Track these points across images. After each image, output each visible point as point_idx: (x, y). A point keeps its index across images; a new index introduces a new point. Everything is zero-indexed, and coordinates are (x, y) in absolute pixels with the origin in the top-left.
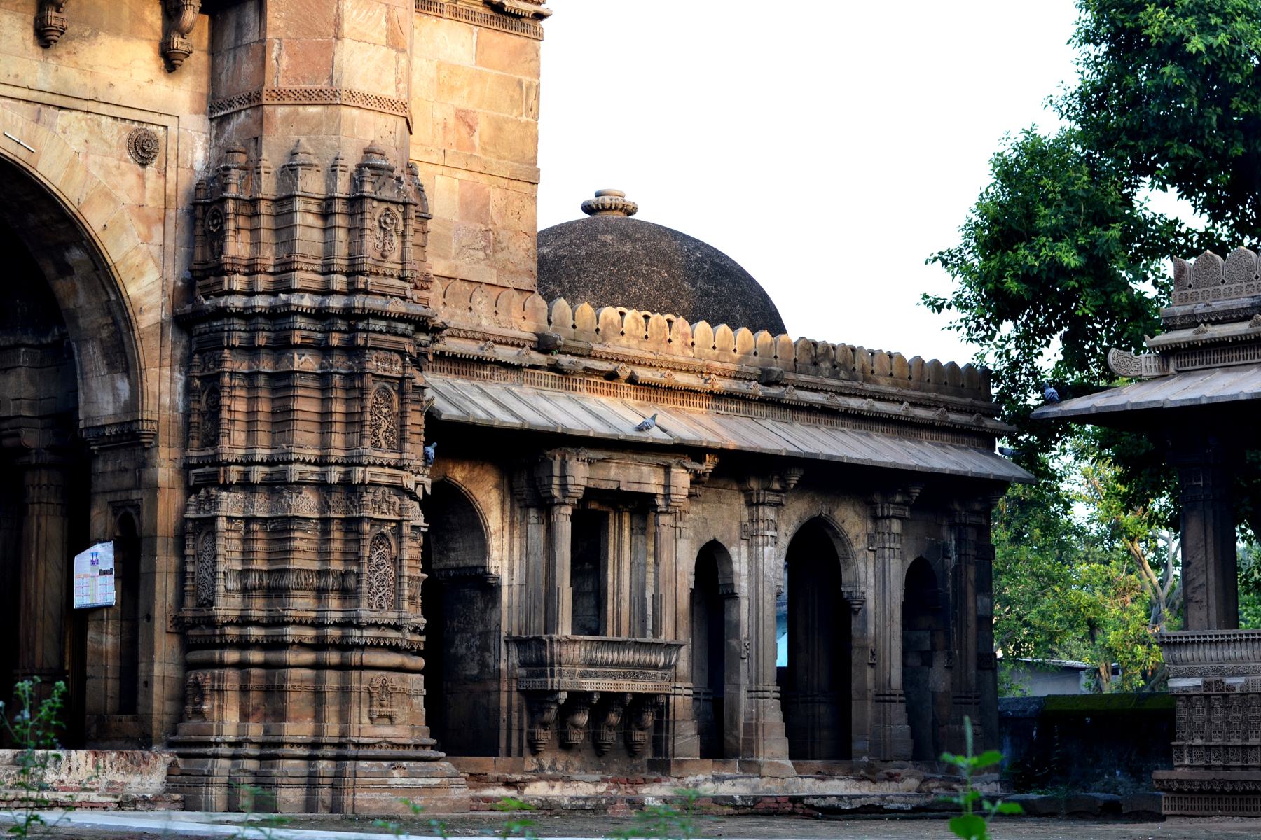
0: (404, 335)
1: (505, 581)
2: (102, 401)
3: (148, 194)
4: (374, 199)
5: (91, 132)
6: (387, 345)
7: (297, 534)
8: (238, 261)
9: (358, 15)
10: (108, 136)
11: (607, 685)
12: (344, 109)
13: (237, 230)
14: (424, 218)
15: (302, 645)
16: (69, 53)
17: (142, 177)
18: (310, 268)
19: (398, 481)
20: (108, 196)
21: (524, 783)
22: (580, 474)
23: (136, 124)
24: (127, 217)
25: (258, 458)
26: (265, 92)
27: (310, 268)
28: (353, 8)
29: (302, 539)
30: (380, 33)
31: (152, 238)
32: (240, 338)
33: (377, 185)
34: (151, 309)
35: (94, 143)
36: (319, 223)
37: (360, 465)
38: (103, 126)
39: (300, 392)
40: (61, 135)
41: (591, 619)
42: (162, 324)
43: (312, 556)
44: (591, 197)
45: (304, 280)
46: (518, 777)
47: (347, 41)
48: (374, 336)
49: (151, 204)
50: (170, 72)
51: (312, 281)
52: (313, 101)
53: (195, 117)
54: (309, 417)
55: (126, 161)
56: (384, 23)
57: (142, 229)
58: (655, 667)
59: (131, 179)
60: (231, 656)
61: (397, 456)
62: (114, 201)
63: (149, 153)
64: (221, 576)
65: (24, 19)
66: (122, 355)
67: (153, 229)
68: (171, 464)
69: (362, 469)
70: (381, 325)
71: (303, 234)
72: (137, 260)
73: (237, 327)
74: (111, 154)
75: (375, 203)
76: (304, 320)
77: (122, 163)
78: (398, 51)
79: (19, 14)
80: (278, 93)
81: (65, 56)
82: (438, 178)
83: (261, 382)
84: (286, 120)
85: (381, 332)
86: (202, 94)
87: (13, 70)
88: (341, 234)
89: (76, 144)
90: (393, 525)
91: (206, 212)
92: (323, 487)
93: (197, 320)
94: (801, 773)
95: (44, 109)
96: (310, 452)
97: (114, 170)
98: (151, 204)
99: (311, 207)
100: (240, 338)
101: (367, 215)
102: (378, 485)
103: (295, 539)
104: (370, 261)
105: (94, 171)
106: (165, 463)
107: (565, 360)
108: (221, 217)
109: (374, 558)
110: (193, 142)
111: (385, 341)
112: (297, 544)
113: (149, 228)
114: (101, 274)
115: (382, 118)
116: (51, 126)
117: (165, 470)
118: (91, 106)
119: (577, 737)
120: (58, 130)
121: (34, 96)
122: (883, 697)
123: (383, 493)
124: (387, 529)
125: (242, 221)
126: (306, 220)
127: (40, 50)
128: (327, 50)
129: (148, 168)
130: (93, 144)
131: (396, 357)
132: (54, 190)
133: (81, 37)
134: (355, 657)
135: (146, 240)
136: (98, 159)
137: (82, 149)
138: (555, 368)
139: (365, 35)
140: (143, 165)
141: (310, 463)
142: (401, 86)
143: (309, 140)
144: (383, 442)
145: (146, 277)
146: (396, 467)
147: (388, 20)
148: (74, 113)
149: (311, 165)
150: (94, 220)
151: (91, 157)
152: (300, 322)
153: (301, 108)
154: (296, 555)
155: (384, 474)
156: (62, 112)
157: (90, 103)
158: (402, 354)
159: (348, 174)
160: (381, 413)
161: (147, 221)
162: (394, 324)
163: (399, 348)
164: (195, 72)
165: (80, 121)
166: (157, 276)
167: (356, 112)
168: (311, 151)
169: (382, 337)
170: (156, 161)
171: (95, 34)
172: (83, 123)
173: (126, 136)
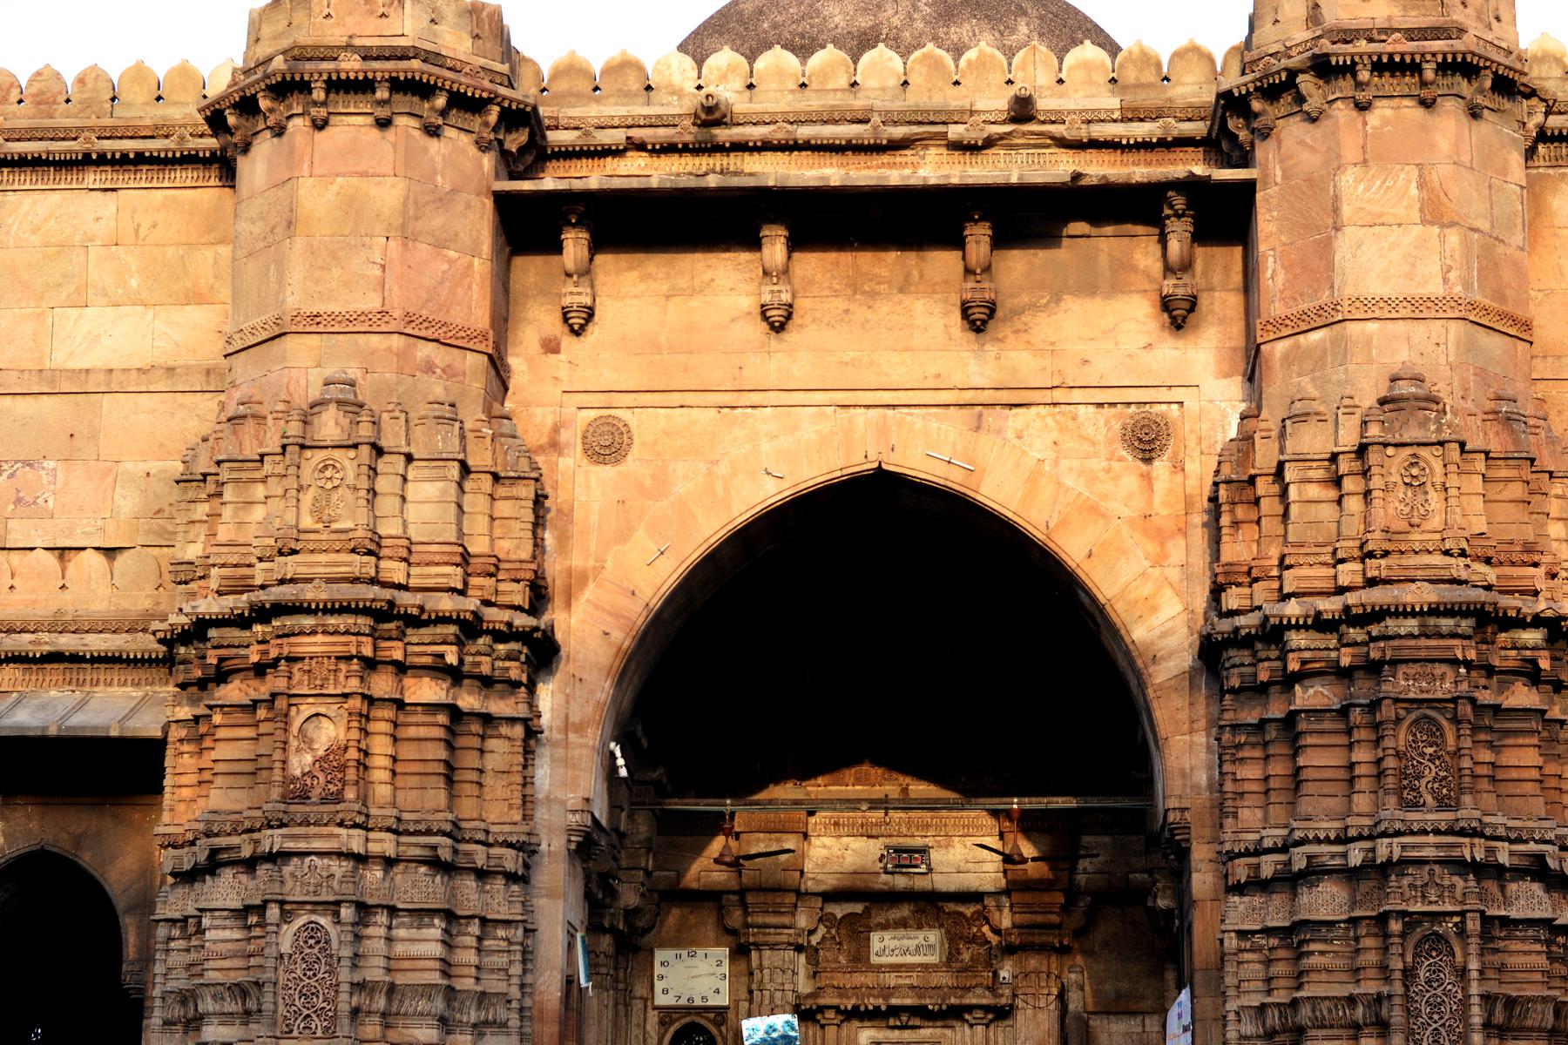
0: (1454, 636)
3: (1157, 499)
4: (1386, 445)
5: (1061, 430)
6: (1423, 654)
7: (1313, 947)
8: (1235, 569)
9: (1366, 190)
10: (1091, 430)
12: (1351, 326)
13: (1236, 524)
16: (1017, 332)
17: (1147, 478)
18: (1311, 560)
19: (1456, 853)
20: (1093, 510)
23: (1133, 407)
24: (1126, 532)
25: (1268, 843)
26: (1259, 327)
27: (1311, 560)
28: (1358, 181)
29: (1322, 953)
30: (1410, 207)
31: (1166, 557)
32: (1241, 675)
33: (1397, 425)
34: (1170, 655)
35: (1067, 444)
36: (1332, 494)
37: (1384, 834)
38: (1081, 419)
39: (1310, 740)
40: (1016, 442)
42: (1192, 674)
43: (1344, 977)
45: (1299, 578)
47: (1348, 230)
48: (1396, 643)
49: (1164, 512)
50: (1179, 327)
51: (1316, 578)
52: (1314, 325)
53: (1226, 381)
54: (1329, 774)
55: (1121, 459)
56: (1414, 191)
57: (1151, 547)
59: (1130, 482)
61: (1449, 816)
62: (1104, 516)
63: (1149, 442)
64: (1231, 1016)
65: (946, 301)
67: (1170, 545)
68: (1213, 866)
69: (1386, 841)
70: (1411, 625)
71: (1301, 514)
72: (1146, 590)
73: (1237, 661)
74: (1096, 455)
75: (1390, 451)
76: (1303, 634)
77: (1116, 465)
78: (1442, 226)
79: (937, 296)
80: (1281, 322)
81: (1011, 339)
83: (1272, 733)
84: (1287, 359)
85: (1411, 636)
86: (1234, 349)
87: (933, 369)
88: (1354, 504)
89: (1039, 448)
90: (1456, 919)
92: (1350, 875)
95: (986, 411)
96: (1325, 825)
97: (1102, 475)
98: (1164, 512)
99: (1312, 474)
100: (1241, 675)
101: (1374, 470)
102: (1420, 862)
103: (1312, 953)
104: (1378, 535)
105: (1069, 481)
106: (1203, 866)
109: (1422, 973)
110: (1224, 416)
111: (1419, 648)
112: (1314, 961)
113: (1162, 544)
115: (1419, 331)
116: (999, 432)
118: (1058, 395)
120: (1010, 434)
121: (968, 397)
123: (1431, 873)
124: (1449, 926)
125: (1241, 512)
126: (1307, 491)
127: (972, 336)
128: (1326, 248)
129: (1156, 463)
130: (1067, 444)
131: (1444, 668)
132: (1010, 515)
133: (1034, 307)
135: (1159, 561)
136: (1075, 463)
137: (1049, 454)
139: (1381, 215)
140: (1148, 461)
141: (1328, 841)
142: (1452, 275)
143: (1313, 380)
144: (1429, 799)
146: (1450, 832)
147: (1421, 186)
148: (1034, 409)
149: (1308, 414)
150: (1073, 549)
151: (1065, 464)
152: (1296, 639)
153: (1301, 338)
154: (1314, 977)
155: (1428, 845)
156: (1015, 411)
157: (1056, 392)
158: (1454, 662)
159: (1358, 416)
160: (1423, 755)
161: (1160, 536)
162: (1432, 621)
163: (1447, 655)
164: (1222, 321)
165: (1044, 418)
166: (1179, 607)
167: (1372, 326)
168: (1314, 393)
169: (1413, 643)
170: (1168, 453)
171: (1057, 299)
172: (1049, 420)
173: (1117, 427)
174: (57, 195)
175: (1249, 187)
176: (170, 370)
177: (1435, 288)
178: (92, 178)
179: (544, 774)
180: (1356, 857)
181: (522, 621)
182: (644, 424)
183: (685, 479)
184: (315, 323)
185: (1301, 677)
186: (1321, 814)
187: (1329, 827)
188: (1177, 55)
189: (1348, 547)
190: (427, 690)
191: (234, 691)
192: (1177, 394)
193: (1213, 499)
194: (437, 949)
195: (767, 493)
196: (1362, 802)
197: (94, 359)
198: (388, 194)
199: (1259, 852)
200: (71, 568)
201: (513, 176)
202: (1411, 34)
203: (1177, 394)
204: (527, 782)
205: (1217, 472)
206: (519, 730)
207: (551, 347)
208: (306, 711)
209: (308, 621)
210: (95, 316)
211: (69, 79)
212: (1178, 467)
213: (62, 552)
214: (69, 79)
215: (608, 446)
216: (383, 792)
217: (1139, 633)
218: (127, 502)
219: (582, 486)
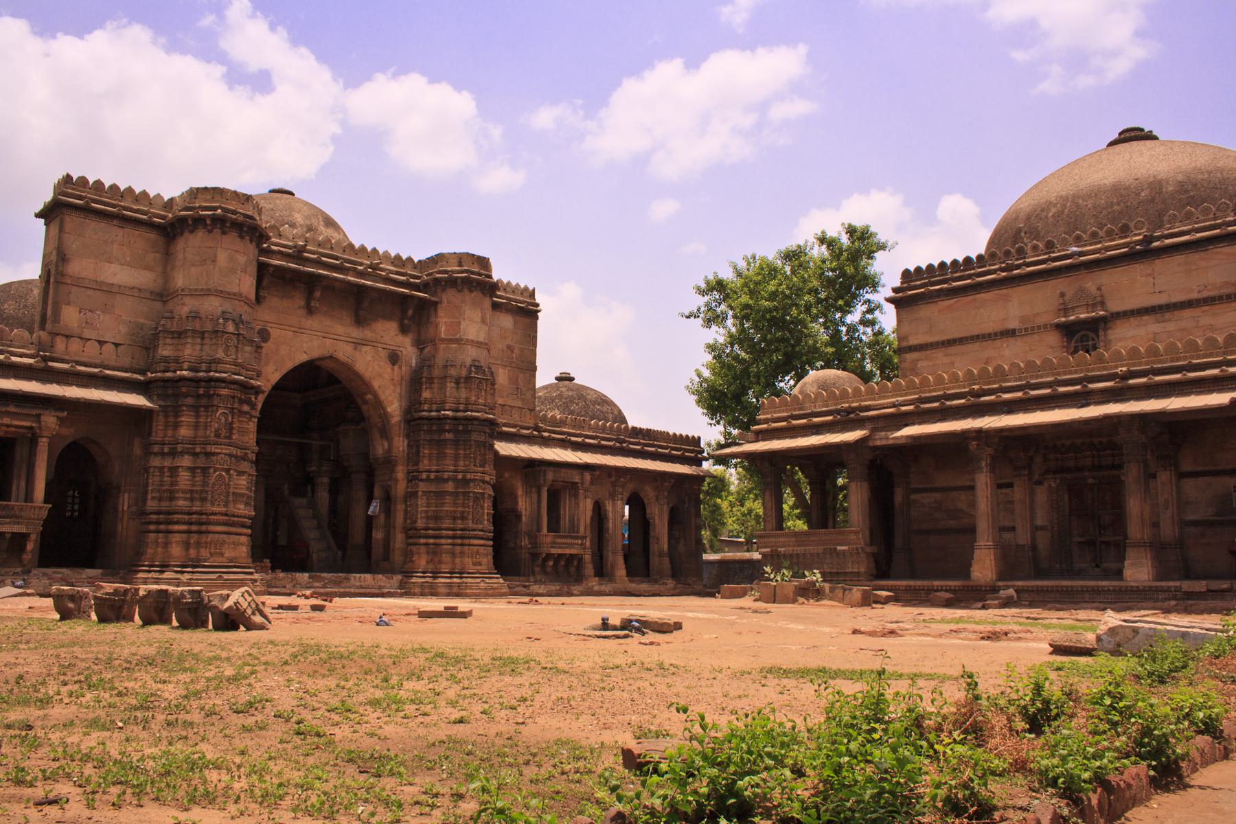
2: (380, 448)
11: (560, 551)
14: (493, 384)
15: (448, 537)
20: (380, 375)
41: (554, 526)
44: (558, 375)
59: (389, 370)
60: (422, 541)
66: (385, 433)
82: (501, 370)
89: (369, 358)
91: (416, 382)
92: (455, 480)
93: (412, 420)
94: (631, 581)
108: (421, 384)
114: (379, 404)
117: (400, 473)
119: (549, 570)
122: (661, 554)
126: (450, 385)
134: (467, 541)
145: (394, 407)
161: (394, 385)
175: (436, 304)
176: (140, 290)
177: (481, 339)
180: (460, 477)
182: (275, 333)
183: (284, 351)
184: (220, 293)
185: (449, 431)
186: (449, 465)
187: (452, 468)
189: (462, 400)
191: (190, 401)
196: (461, 463)
197: (115, 280)
199: (429, 471)
210: (114, 267)
211: (107, 186)
212: (400, 367)
213: (101, 343)
214: (107, 186)
217: (389, 410)
218: (123, 329)
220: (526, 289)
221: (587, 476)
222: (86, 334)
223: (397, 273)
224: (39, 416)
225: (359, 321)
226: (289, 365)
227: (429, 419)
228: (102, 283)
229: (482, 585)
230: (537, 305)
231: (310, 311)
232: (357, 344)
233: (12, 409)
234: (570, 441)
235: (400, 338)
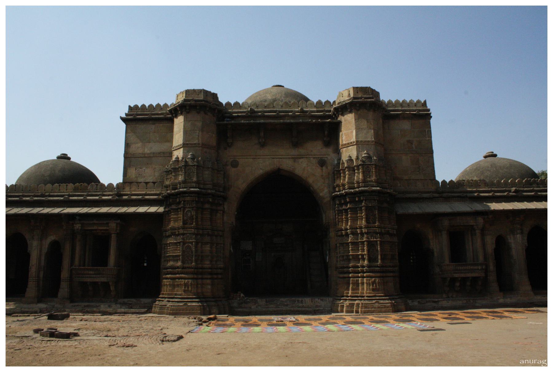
1: (435, 250)
11: (463, 275)
17: (322, 170)
21: (438, 301)
22: (446, 223)
46: (436, 300)
58: (478, 269)
107: (445, 195)
118: (308, 156)
138: (441, 197)
140: (322, 166)
150: (310, 180)
158: (375, 200)
174: (145, 125)
176: (164, 153)
178: (150, 122)
179: (225, 218)
181: (222, 194)
188: (325, 102)
190: (207, 206)
192: (326, 156)
193: (334, 173)
194: (209, 249)
195: (261, 172)
198: (199, 124)
200: (148, 185)
201: (219, 121)
202: (366, 98)
203: (326, 156)
204: (223, 219)
205: (334, 168)
206: (222, 212)
207: (226, 149)
208: (187, 210)
209: (187, 195)
212: (327, 167)
213: (147, 183)
215: (235, 164)
216: (200, 223)
219: (232, 171)
220: (419, 102)
221: (480, 220)
222: (140, 180)
223: (318, 112)
224: (108, 224)
225: (296, 145)
226: (251, 178)
227: (342, 195)
228: (145, 154)
229: (377, 305)
230: (429, 110)
231: (263, 145)
232: (295, 159)
233: (95, 222)
234: (466, 197)
235: (325, 150)
